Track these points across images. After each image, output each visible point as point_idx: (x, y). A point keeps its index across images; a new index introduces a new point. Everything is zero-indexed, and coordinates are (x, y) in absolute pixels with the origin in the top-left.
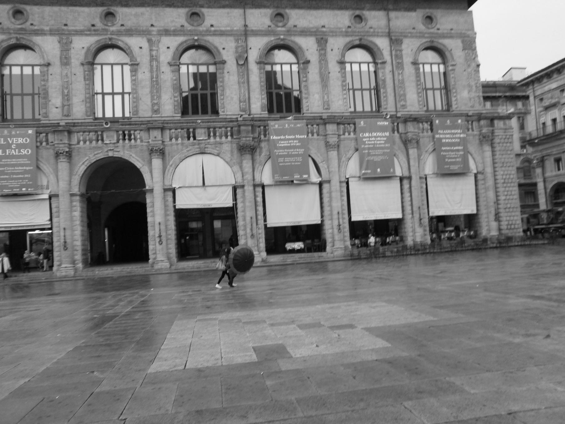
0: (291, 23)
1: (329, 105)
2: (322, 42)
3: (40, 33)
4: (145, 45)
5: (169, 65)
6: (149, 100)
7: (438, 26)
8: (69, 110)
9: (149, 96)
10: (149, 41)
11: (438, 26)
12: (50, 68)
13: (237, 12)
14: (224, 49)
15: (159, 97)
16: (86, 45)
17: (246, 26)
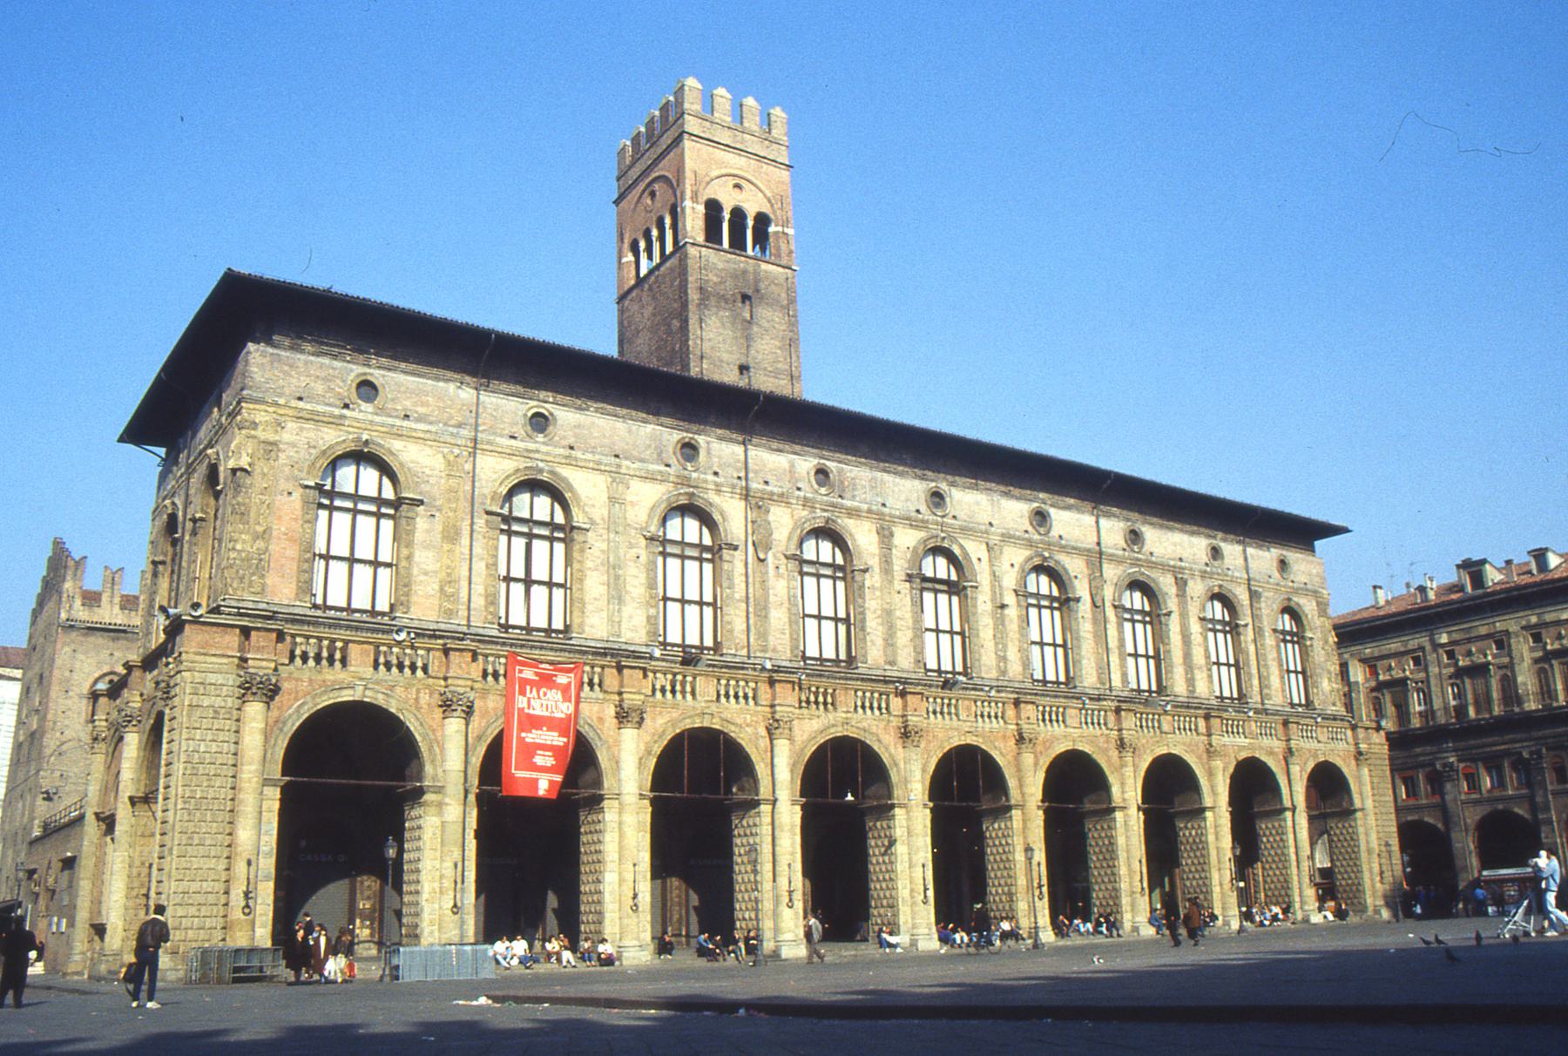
0: (1146, 548)
1: (1194, 686)
2: (1181, 584)
3: (853, 513)
4: (984, 555)
5: (1014, 594)
6: (993, 649)
7: (1292, 577)
8: (895, 654)
9: (992, 644)
10: (989, 548)
11: (1292, 577)
12: (867, 575)
13: (1088, 520)
14: (1076, 577)
15: (1005, 647)
16: (912, 544)
17: (1098, 544)
